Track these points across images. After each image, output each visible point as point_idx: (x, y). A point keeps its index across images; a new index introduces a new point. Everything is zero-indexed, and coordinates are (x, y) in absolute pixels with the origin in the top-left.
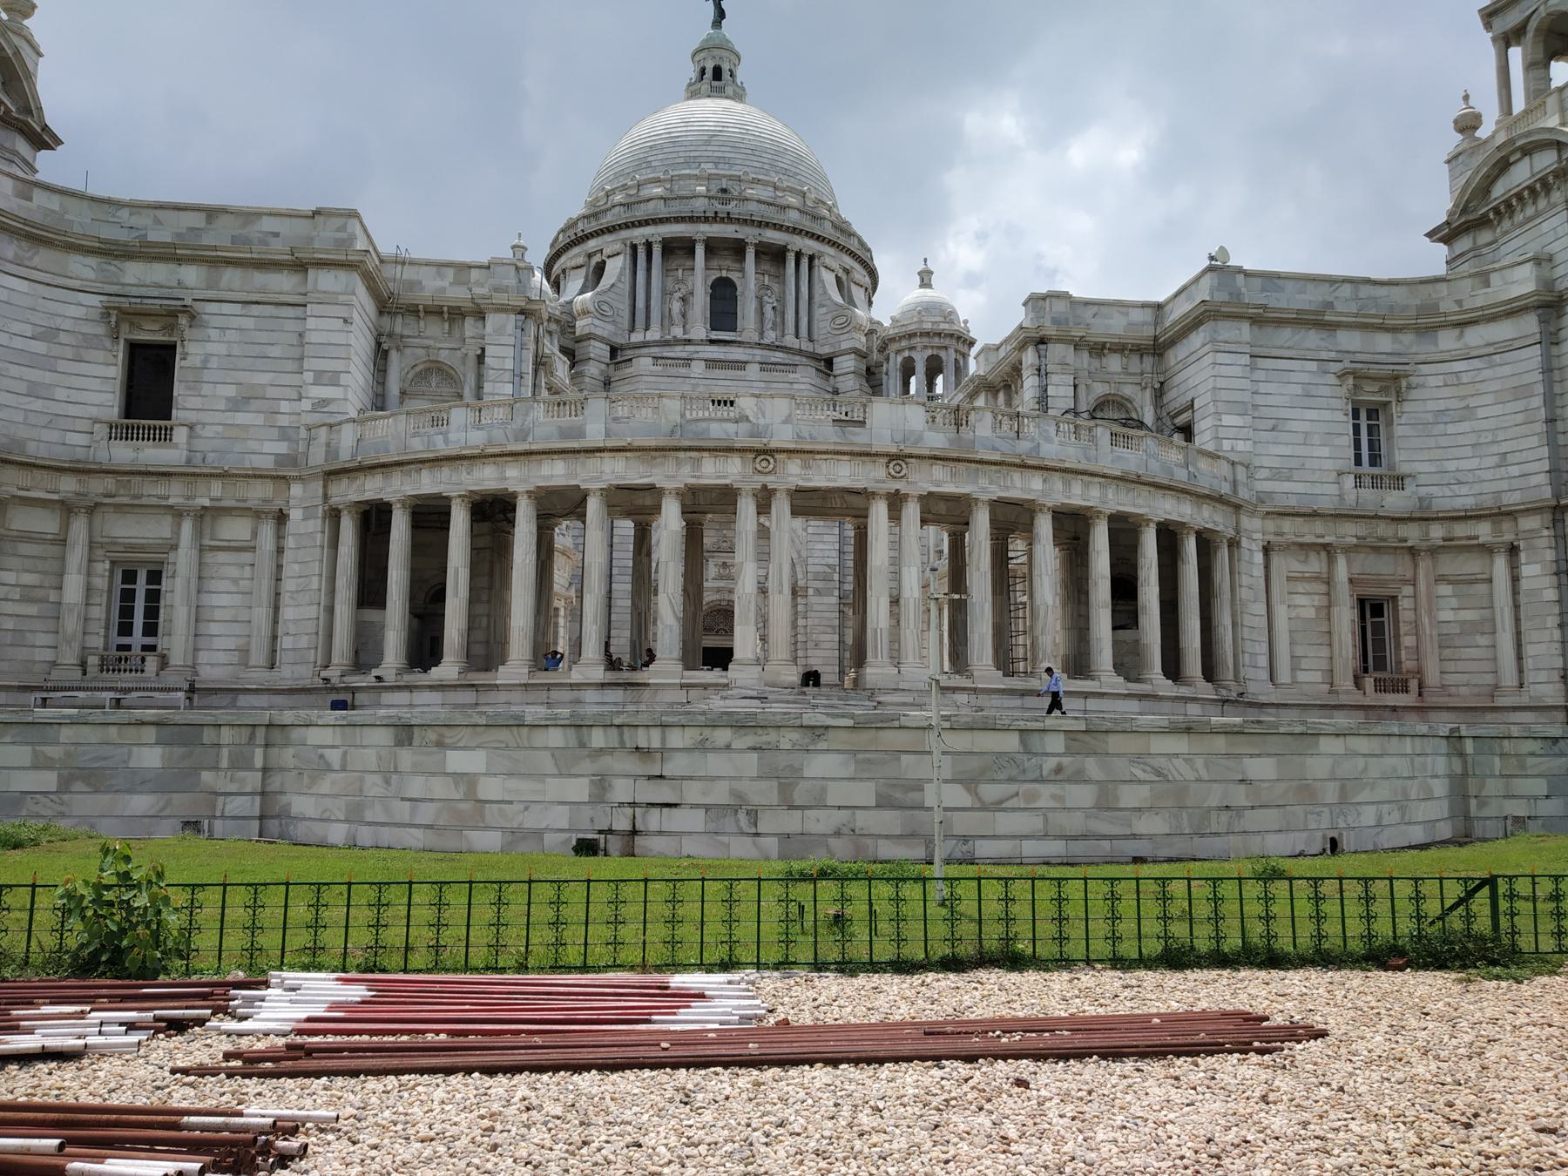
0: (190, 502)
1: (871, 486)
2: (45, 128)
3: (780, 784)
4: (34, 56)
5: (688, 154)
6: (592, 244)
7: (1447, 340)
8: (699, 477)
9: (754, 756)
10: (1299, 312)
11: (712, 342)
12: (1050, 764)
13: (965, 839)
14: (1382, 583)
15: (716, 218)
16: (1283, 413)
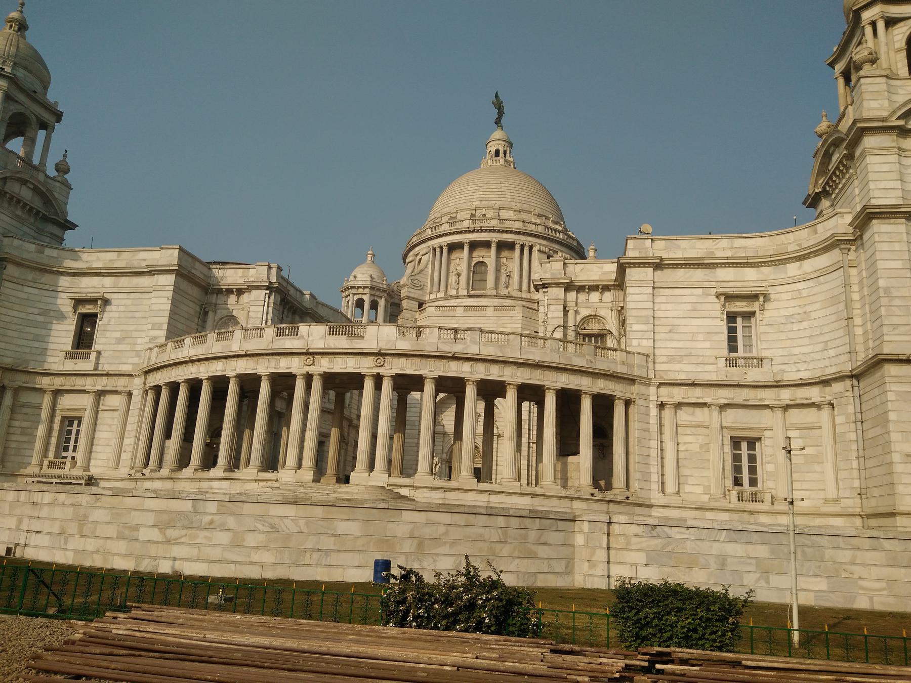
0: (94, 388)
1: (363, 371)
2: (66, 220)
3: (79, 524)
4: (66, 189)
5: (467, 198)
6: (417, 249)
7: (793, 269)
8: (279, 369)
9: (71, 509)
10: (686, 259)
11: (470, 296)
12: (207, 518)
13: (156, 558)
14: (751, 429)
15: (474, 231)
16: (676, 322)
